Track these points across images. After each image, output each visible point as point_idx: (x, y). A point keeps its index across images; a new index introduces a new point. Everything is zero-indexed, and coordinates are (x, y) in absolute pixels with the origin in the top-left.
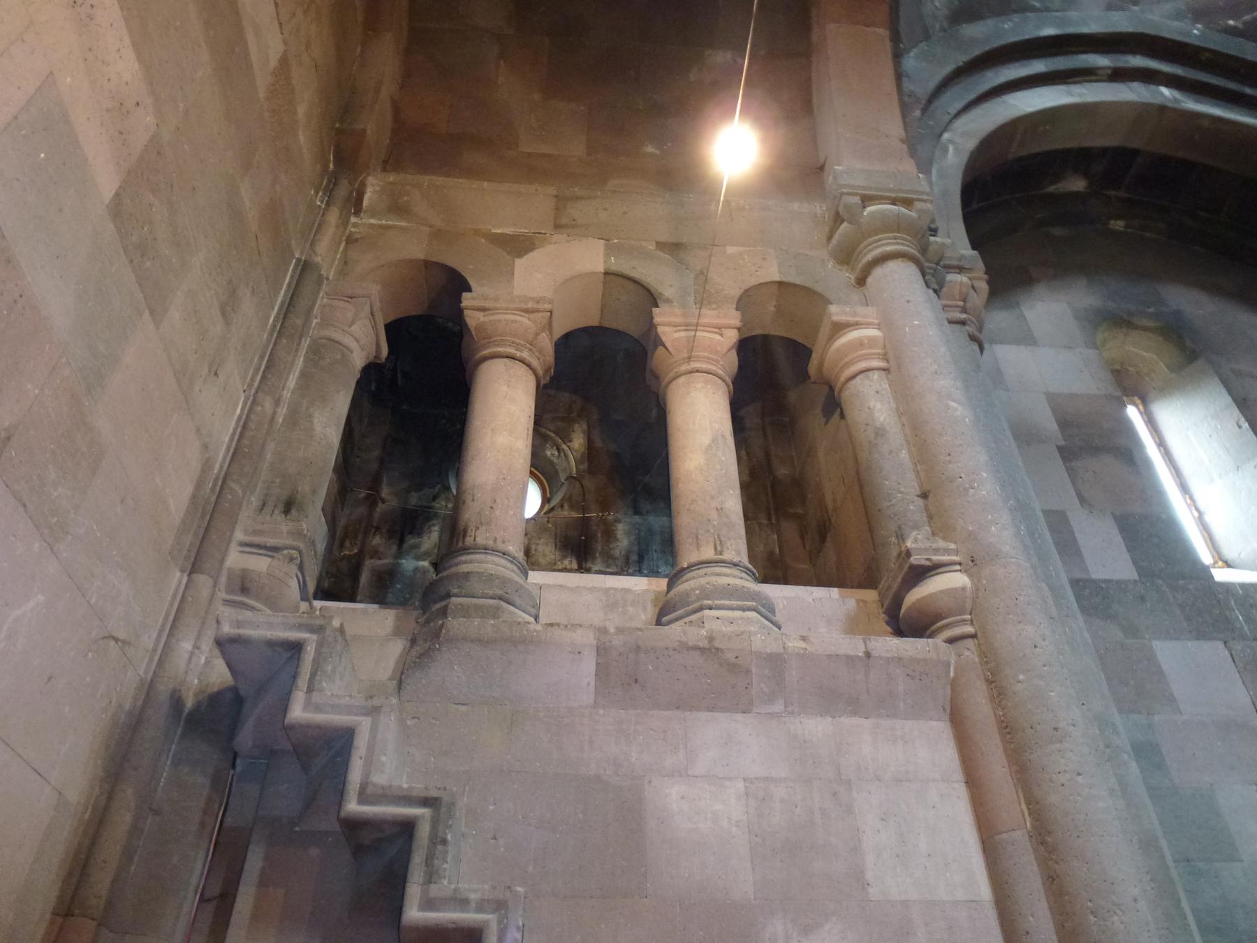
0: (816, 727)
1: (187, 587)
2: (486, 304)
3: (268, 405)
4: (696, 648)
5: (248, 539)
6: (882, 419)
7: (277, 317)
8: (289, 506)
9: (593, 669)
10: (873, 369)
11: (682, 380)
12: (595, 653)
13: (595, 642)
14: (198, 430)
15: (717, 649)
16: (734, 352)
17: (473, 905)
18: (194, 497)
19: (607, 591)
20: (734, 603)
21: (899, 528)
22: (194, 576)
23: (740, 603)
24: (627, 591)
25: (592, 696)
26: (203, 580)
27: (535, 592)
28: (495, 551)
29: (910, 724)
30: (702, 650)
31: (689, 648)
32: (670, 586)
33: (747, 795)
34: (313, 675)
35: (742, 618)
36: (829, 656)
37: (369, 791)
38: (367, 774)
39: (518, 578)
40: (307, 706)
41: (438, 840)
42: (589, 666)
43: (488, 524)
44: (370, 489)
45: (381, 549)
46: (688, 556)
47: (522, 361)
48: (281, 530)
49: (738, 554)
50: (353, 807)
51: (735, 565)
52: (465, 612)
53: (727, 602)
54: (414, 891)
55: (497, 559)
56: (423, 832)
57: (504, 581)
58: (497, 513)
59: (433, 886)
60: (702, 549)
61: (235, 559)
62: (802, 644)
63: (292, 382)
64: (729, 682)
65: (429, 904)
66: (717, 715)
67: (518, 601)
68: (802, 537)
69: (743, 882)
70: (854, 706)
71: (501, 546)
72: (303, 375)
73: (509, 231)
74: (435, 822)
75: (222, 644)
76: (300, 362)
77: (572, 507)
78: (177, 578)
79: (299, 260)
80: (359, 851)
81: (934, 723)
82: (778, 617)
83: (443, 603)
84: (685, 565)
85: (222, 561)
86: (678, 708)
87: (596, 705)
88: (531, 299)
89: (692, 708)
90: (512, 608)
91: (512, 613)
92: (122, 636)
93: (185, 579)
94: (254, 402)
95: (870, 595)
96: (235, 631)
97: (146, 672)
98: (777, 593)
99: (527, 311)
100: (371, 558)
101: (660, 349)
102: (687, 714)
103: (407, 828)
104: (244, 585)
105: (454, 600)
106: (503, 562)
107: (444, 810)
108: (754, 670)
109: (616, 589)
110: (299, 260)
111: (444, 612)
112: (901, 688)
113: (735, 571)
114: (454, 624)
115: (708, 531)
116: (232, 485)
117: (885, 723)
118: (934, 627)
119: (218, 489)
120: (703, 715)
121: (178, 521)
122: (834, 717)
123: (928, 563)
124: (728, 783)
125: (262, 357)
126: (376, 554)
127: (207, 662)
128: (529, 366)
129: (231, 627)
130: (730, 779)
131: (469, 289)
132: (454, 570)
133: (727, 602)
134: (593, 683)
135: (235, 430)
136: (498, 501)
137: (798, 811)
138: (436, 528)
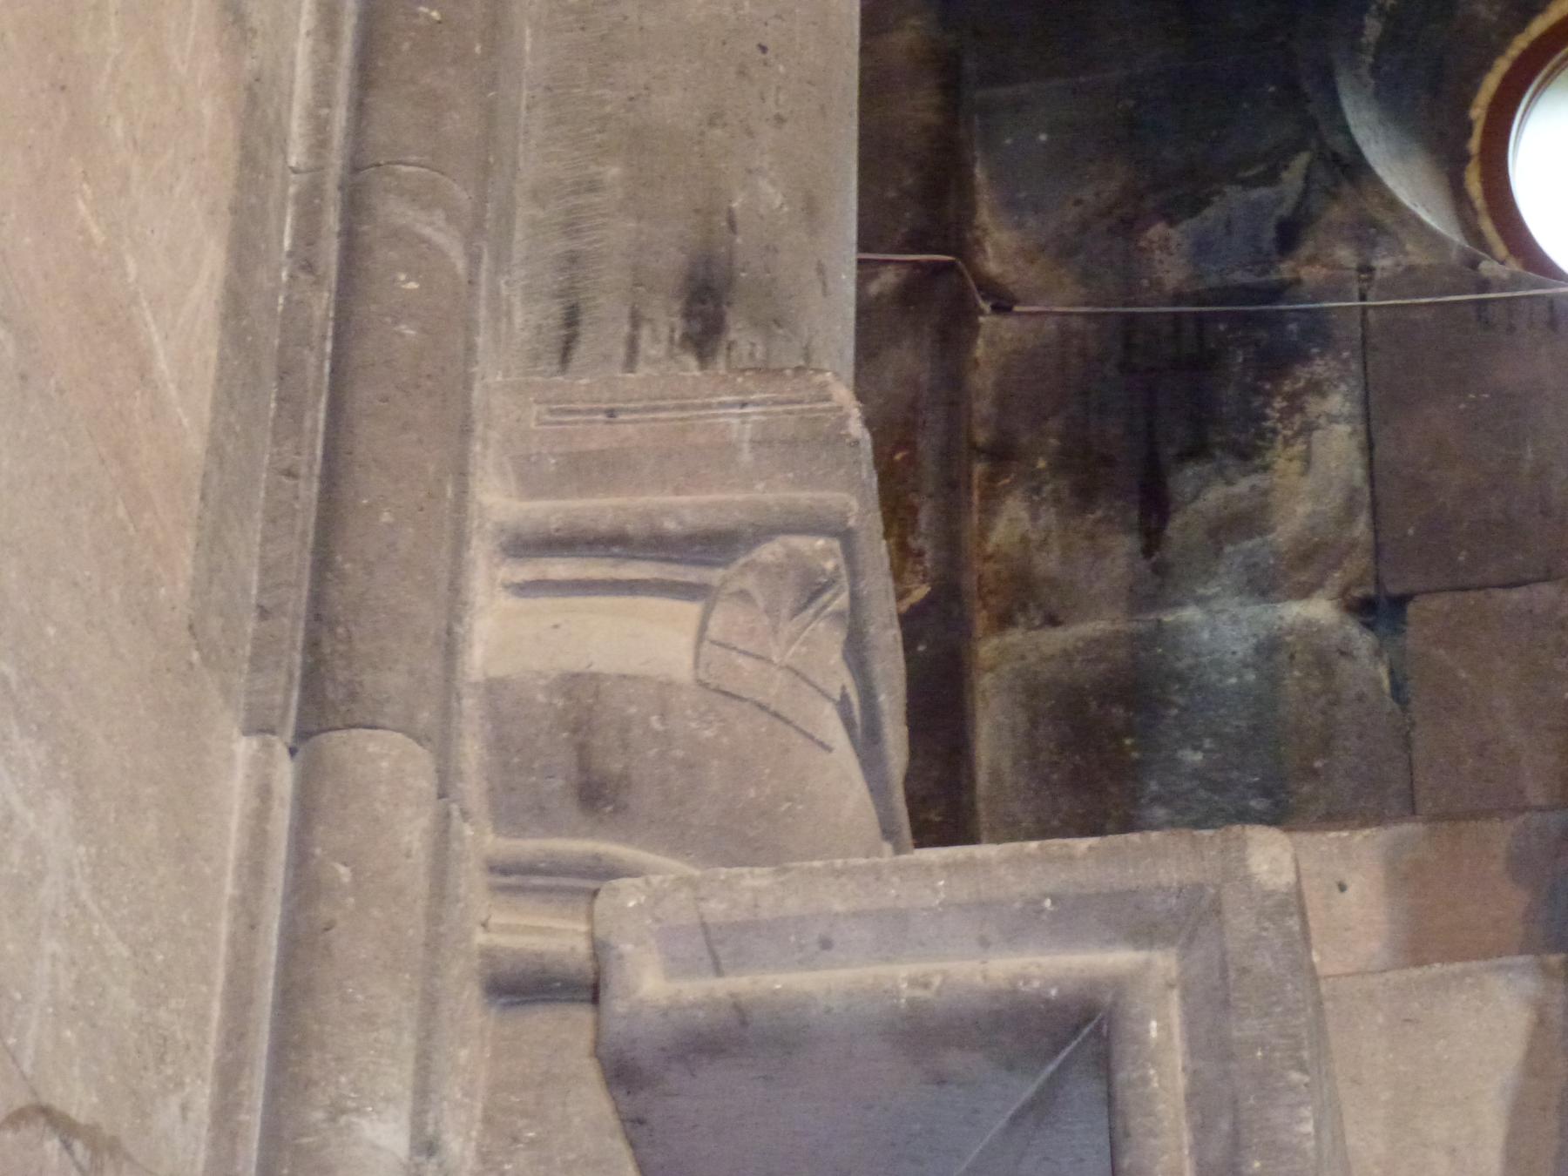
1: (306, 812)
5: (549, 511)
8: (707, 307)
18: (235, 303)
26: (382, 759)
44: (916, 242)
45: (1048, 563)
61: (509, 633)
78: (243, 769)
85: (450, 647)
92: (80, 1102)
93: (285, 774)
96: (700, 989)
100: (1004, 621)
104: (588, 766)
119: (330, 250)
121: (196, 445)
126: (1023, 596)
129: (676, 967)
138: (1337, 402)
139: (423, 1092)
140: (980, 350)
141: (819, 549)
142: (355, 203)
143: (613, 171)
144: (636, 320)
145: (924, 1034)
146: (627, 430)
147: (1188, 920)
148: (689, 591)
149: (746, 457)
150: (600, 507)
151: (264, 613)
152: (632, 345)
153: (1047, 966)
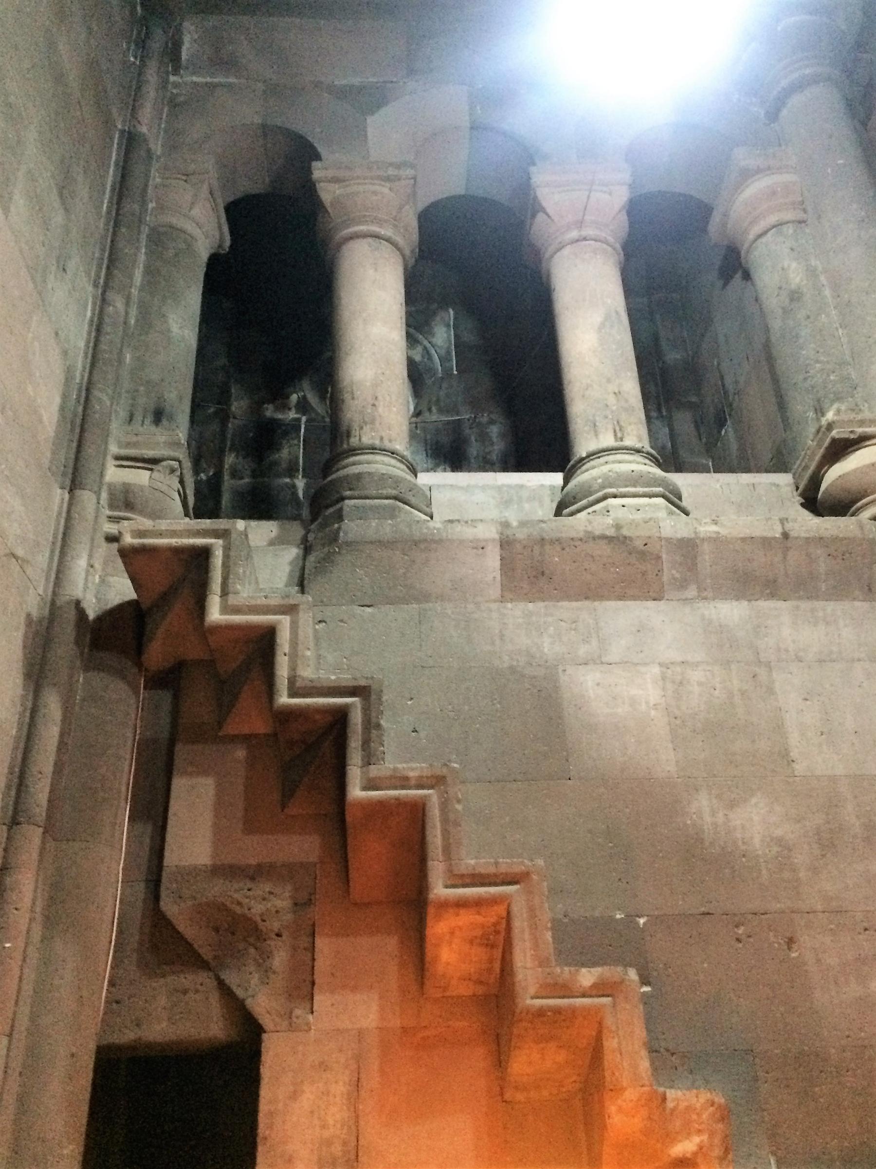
0: (731, 612)
2: (341, 174)
4: (603, 537)
5: (124, 452)
6: (798, 280)
7: (110, 202)
8: (159, 416)
9: (497, 564)
10: (788, 222)
11: (566, 251)
13: (497, 537)
14: (57, 334)
15: (625, 537)
16: (624, 213)
18: (62, 409)
19: (499, 488)
20: (640, 490)
21: (819, 400)
22: (78, 492)
23: (646, 490)
24: (522, 486)
25: (499, 592)
28: (383, 450)
29: (831, 607)
32: (566, 481)
33: (664, 678)
35: (649, 505)
36: (743, 539)
38: (293, 668)
39: (409, 477)
41: (371, 725)
42: (493, 560)
43: (373, 422)
44: (219, 403)
45: (240, 467)
46: (583, 445)
47: (388, 240)
49: (640, 440)
50: (284, 699)
51: (638, 451)
52: (362, 514)
54: (355, 774)
55: (387, 459)
56: (356, 718)
57: (397, 481)
58: (380, 410)
60: (601, 437)
62: (714, 528)
63: (138, 276)
64: (636, 570)
67: (413, 500)
68: (697, 427)
69: (666, 761)
70: (771, 588)
71: (387, 445)
72: (149, 271)
74: (366, 710)
75: (128, 555)
76: (142, 258)
77: (440, 411)
78: (59, 496)
81: (857, 604)
82: (684, 504)
83: (338, 506)
84: (584, 455)
85: (102, 475)
86: (587, 598)
88: (391, 164)
89: (601, 597)
90: (407, 507)
91: (407, 512)
92: (20, 552)
93: (67, 496)
95: (784, 480)
96: (137, 541)
97: (45, 591)
98: (680, 480)
99: (388, 179)
101: (540, 217)
102: (596, 603)
103: (341, 716)
105: (347, 502)
106: (393, 462)
107: (373, 697)
108: (664, 556)
110: (122, 132)
111: (339, 516)
113: (637, 457)
114: (351, 528)
115: (606, 417)
117: (805, 605)
118: (859, 504)
119: (82, 400)
121: (52, 434)
122: (749, 601)
123: (852, 436)
124: (643, 669)
127: (103, 581)
129: (133, 537)
130: (646, 664)
131: (318, 157)
134: (499, 578)
136: (380, 398)
137: (717, 693)
139: (90, 556)
140: (230, 425)
141: (175, 464)
142: (88, 390)
143: (142, 388)
145: (177, 551)
146: (140, 438)
147: (224, 534)
148: (151, 470)
151: (65, 467)
152: (143, 422)
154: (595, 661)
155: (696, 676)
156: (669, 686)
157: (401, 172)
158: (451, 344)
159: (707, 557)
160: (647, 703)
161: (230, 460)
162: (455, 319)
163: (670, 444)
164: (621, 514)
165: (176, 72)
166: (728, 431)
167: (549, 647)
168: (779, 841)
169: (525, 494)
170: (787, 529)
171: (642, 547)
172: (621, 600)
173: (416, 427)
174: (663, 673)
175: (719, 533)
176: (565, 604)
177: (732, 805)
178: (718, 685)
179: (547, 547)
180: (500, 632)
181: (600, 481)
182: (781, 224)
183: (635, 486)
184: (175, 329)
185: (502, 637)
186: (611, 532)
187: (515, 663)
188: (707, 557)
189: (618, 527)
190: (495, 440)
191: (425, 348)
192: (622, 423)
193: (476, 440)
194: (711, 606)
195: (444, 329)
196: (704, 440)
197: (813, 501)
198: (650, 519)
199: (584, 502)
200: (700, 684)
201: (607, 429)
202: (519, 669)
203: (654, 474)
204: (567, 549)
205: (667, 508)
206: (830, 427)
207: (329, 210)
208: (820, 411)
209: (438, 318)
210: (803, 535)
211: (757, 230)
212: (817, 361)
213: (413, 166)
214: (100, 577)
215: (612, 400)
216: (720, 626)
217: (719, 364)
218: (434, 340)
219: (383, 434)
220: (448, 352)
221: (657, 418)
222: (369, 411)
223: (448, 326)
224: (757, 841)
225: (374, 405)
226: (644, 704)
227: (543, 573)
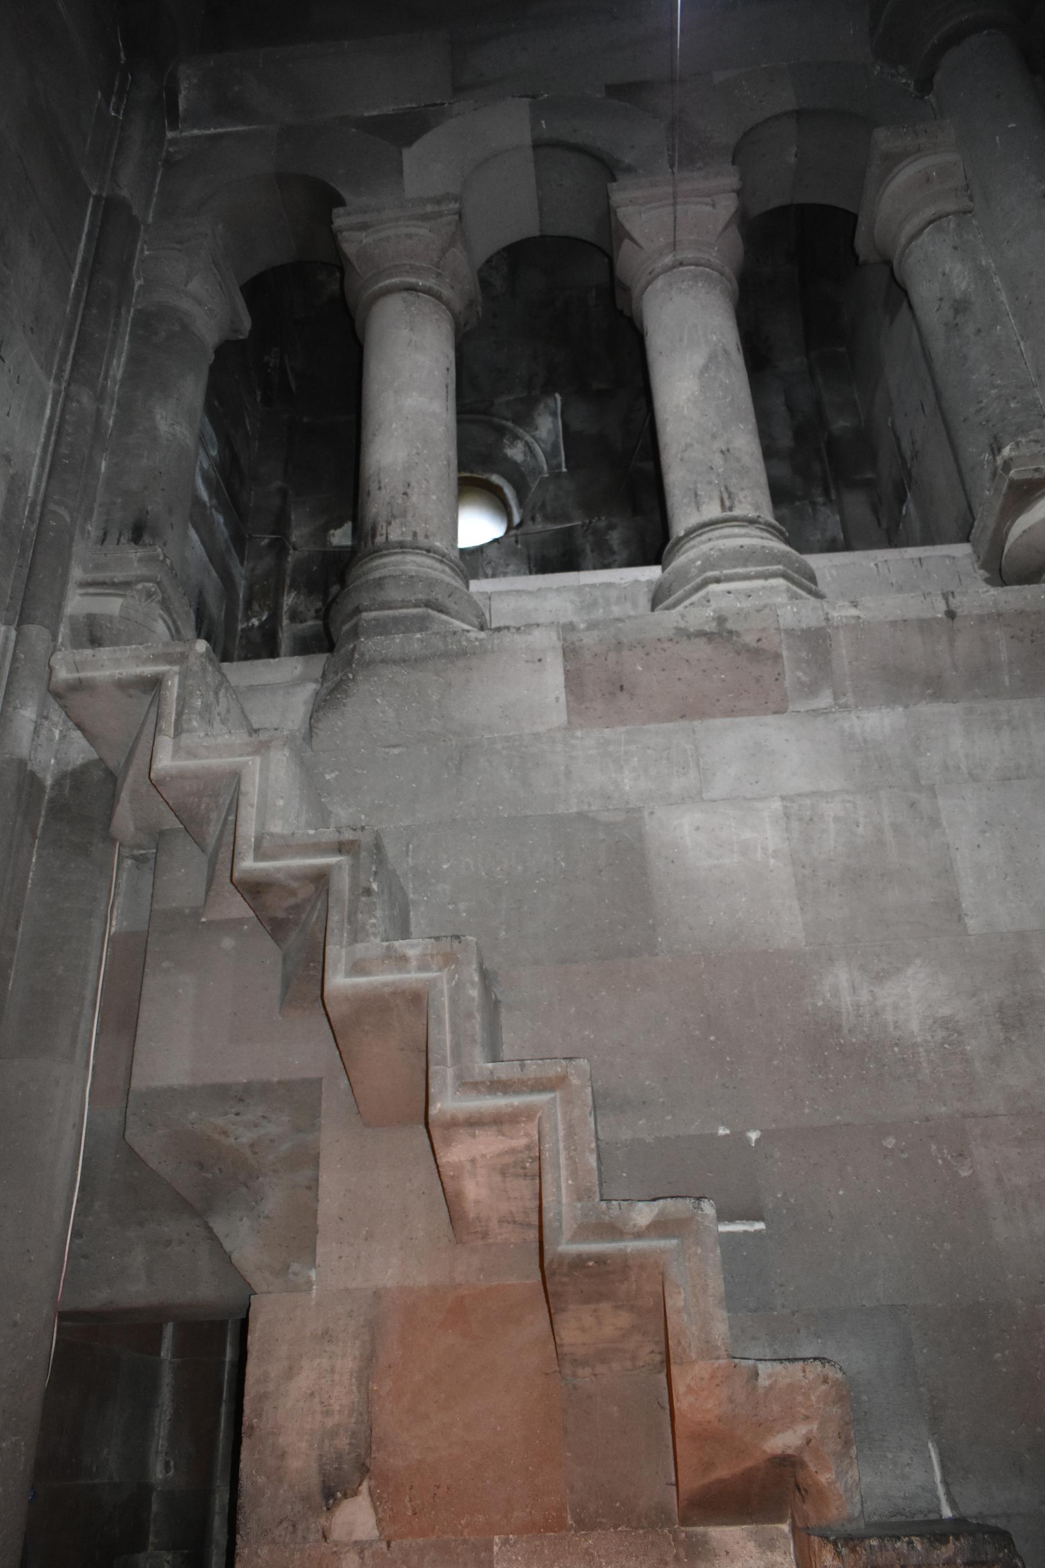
0: (879, 722)
1: (17, 642)
3: (86, 399)
4: (701, 634)
6: (963, 286)
9: (561, 679)
10: (947, 215)
11: (659, 283)
12: (560, 658)
13: (559, 644)
15: (730, 632)
17: (414, 963)
19: (580, 589)
20: (752, 569)
22: (26, 627)
23: (760, 569)
24: (610, 585)
26: (33, 630)
27: (482, 603)
30: (708, 636)
31: (689, 636)
33: (787, 816)
34: (179, 714)
35: (763, 588)
36: (893, 624)
37: (265, 844)
38: (262, 823)
39: (457, 583)
40: (176, 750)
42: (554, 675)
43: (404, 514)
44: (273, 533)
45: (301, 608)
47: (428, 291)
48: (131, 562)
49: (757, 508)
50: (248, 864)
51: (752, 522)
52: (383, 628)
53: (740, 570)
54: (337, 953)
55: (419, 559)
57: (431, 583)
58: (414, 499)
59: (359, 946)
60: (704, 508)
62: (854, 612)
63: (118, 368)
64: (747, 673)
65: (357, 968)
66: (737, 720)
67: (449, 603)
68: (875, 511)
69: (788, 925)
71: (422, 541)
72: (134, 360)
73: (388, 109)
77: (547, 518)
79: (98, 198)
80: (277, 928)
82: (822, 587)
83: (354, 621)
84: (682, 533)
85: (59, 607)
86: (683, 717)
87: (570, 726)
89: (703, 715)
90: (444, 617)
93: (13, 634)
94: (68, 398)
95: (962, 550)
101: (627, 243)
106: (428, 561)
108: (785, 653)
109: (593, 586)
110: (98, 198)
112: (1004, 656)
113: (752, 530)
114: (370, 645)
115: (710, 483)
116: (52, 507)
119: (37, 515)
120: (719, 722)
123: (1037, 476)
124: (759, 805)
125: (69, 338)
127: (63, 737)
128: (438, 296)
129: (69, 671)
130: (760, 798)
131: (341, 202)
132: (363, 580)
133: (740, 570)
135: (48, 437)
136: (413, 484)
137: (861, 829)
140: (290, 559)
143: (119, 500)
144: (120, 535)
149: (136, 564)
150: (100, 576)
152: (119, 541)
153: (149, 670)
154: (694, 798)
155: (831, 809)
156: (795, 824)
157: (444, 208)
158: (557, 436)
159: (844, 652)
160: (764, 849)
161: (288, 600)
162: (563, 405)
163: (841, 536)
164: (725, 604)
165: (174, 126)
166: (910, 508)
167: (630, 783)
168: (946, 1023)
169: (613, 594)
170: (952, 607)
171: (754, 644)
172: (730, 716)
173: (517, 542)
174: (785, 807)
175: (859, 617)
176: (652, 727)
177: (880, 978)
178: (861, 820)
179: (626, 653)
180: (567, 767)
181: (699, 563)
182: (940, 217)
183: (745, 566)
184: (163, 427)
185: (568, 773)
186: (712, 627)
187: (586, 808)
188: (844, 652)
189: (721, 620)
190: (616, 547)
191: (527, 444)
192: (732, 490)
193: (592, 551)
194: (853, 716)
195: (550, 419)
196: (884, 525)
197: (1000, 571)
198: (765, 606)
199: (680, 593)
200: (837, 819)
201: (711, 498)
202: (591, 815)
203: (772, 549)
204: (653, 654)
205: (788, 590)
206: (1007, 465)
207: (355, 263)
208: (996, 448)
209: (542, 406)
210: (976, 612)
211: (909, 229)
212: (993, 387)
213: (457, 199)
214: (61, 731)
215: (718, 460)
216: (865, 741)
217: (893, 423)
218: (537, 433)
219: (418, 530)
220: (555, 446)
221: (824, 504)
222: (400, 501)
223: (554, 414)
224: (915, 1026)
225: (405, 494)
226: (759, 850)
227: (622, 688)
